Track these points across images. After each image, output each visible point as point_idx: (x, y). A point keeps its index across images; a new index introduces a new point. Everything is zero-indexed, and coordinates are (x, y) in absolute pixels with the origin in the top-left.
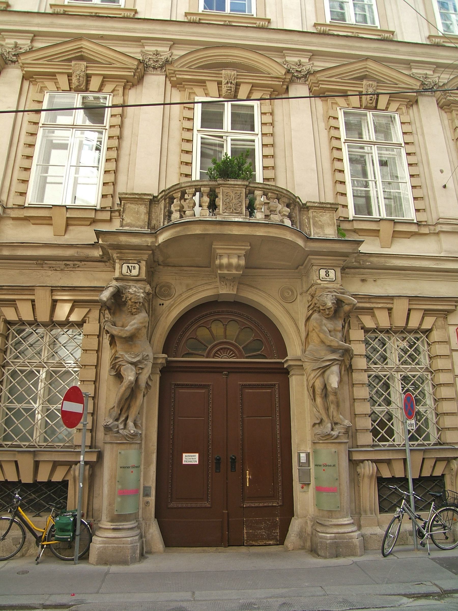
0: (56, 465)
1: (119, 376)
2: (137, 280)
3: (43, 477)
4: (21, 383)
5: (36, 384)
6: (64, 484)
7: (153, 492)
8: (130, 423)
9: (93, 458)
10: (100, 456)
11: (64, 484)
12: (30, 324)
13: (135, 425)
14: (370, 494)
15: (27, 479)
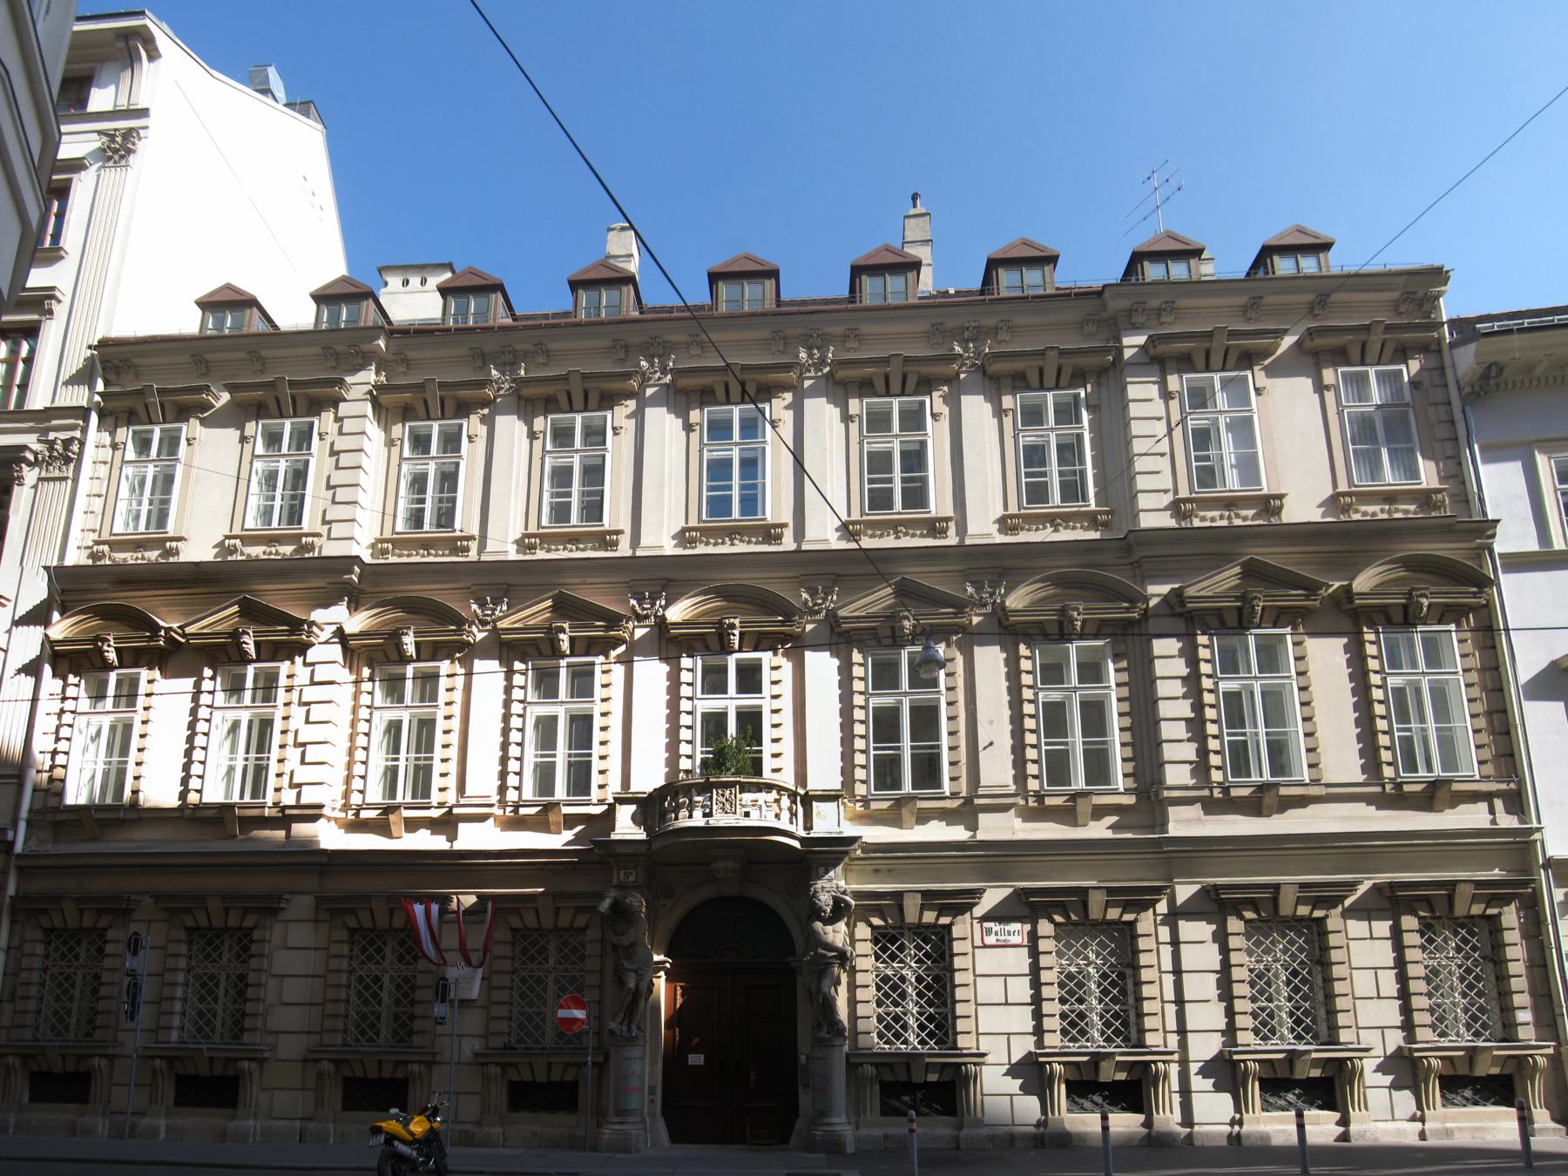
0: (567, 1065)
1: (621, 983)
2: (636, 887)
3: (555, 1077)
4: (531, 988)
5: (545, 990)
6: (575, 1084)
7: (659, 1091)
8: (634, 1027)
9: (600, 1059)
10: (607, 1058)
11: (575, 1084)
12: (535, 930)
13: (639, 1028)
14: (873, 1096)
15: (541, 1078)
